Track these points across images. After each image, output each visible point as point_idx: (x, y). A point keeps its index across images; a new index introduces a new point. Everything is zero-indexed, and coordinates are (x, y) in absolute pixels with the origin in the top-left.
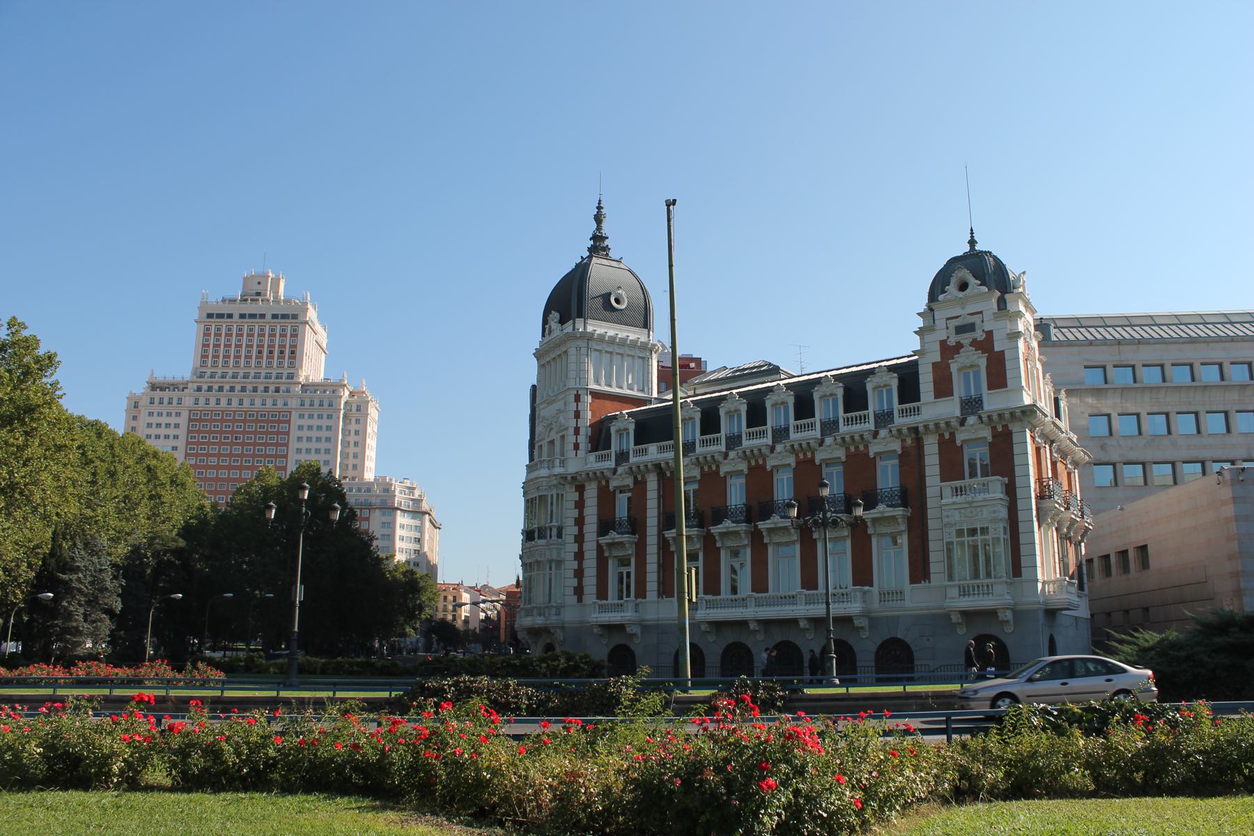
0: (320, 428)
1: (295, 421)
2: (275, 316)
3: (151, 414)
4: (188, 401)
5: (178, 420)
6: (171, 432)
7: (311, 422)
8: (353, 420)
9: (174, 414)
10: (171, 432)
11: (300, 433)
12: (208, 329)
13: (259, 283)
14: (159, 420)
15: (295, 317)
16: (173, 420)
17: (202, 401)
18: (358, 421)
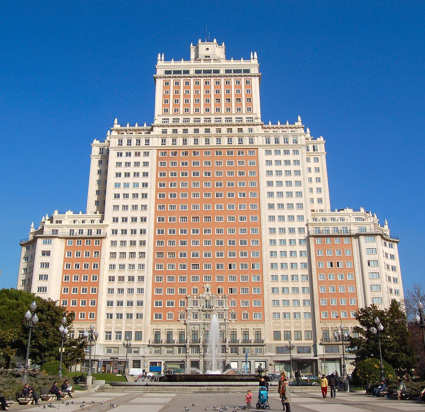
0: (287, 162)
1: (263, 157)
2: (227, 71)
3: (120, 155)
4: (156, 142)
5: (146, 159)
6: (141, 169)
7: (278, 158)
8: (312, 159)
9: (142, 154)
10: (141, 169)
11: (269, 168)
12: (167, 84)
13: (207, 49)
14: (128, 159)
15: (247, 71)
16: (142, 159)
17: (169, 142)
18: (316, 160)
